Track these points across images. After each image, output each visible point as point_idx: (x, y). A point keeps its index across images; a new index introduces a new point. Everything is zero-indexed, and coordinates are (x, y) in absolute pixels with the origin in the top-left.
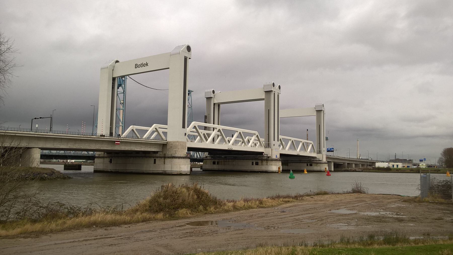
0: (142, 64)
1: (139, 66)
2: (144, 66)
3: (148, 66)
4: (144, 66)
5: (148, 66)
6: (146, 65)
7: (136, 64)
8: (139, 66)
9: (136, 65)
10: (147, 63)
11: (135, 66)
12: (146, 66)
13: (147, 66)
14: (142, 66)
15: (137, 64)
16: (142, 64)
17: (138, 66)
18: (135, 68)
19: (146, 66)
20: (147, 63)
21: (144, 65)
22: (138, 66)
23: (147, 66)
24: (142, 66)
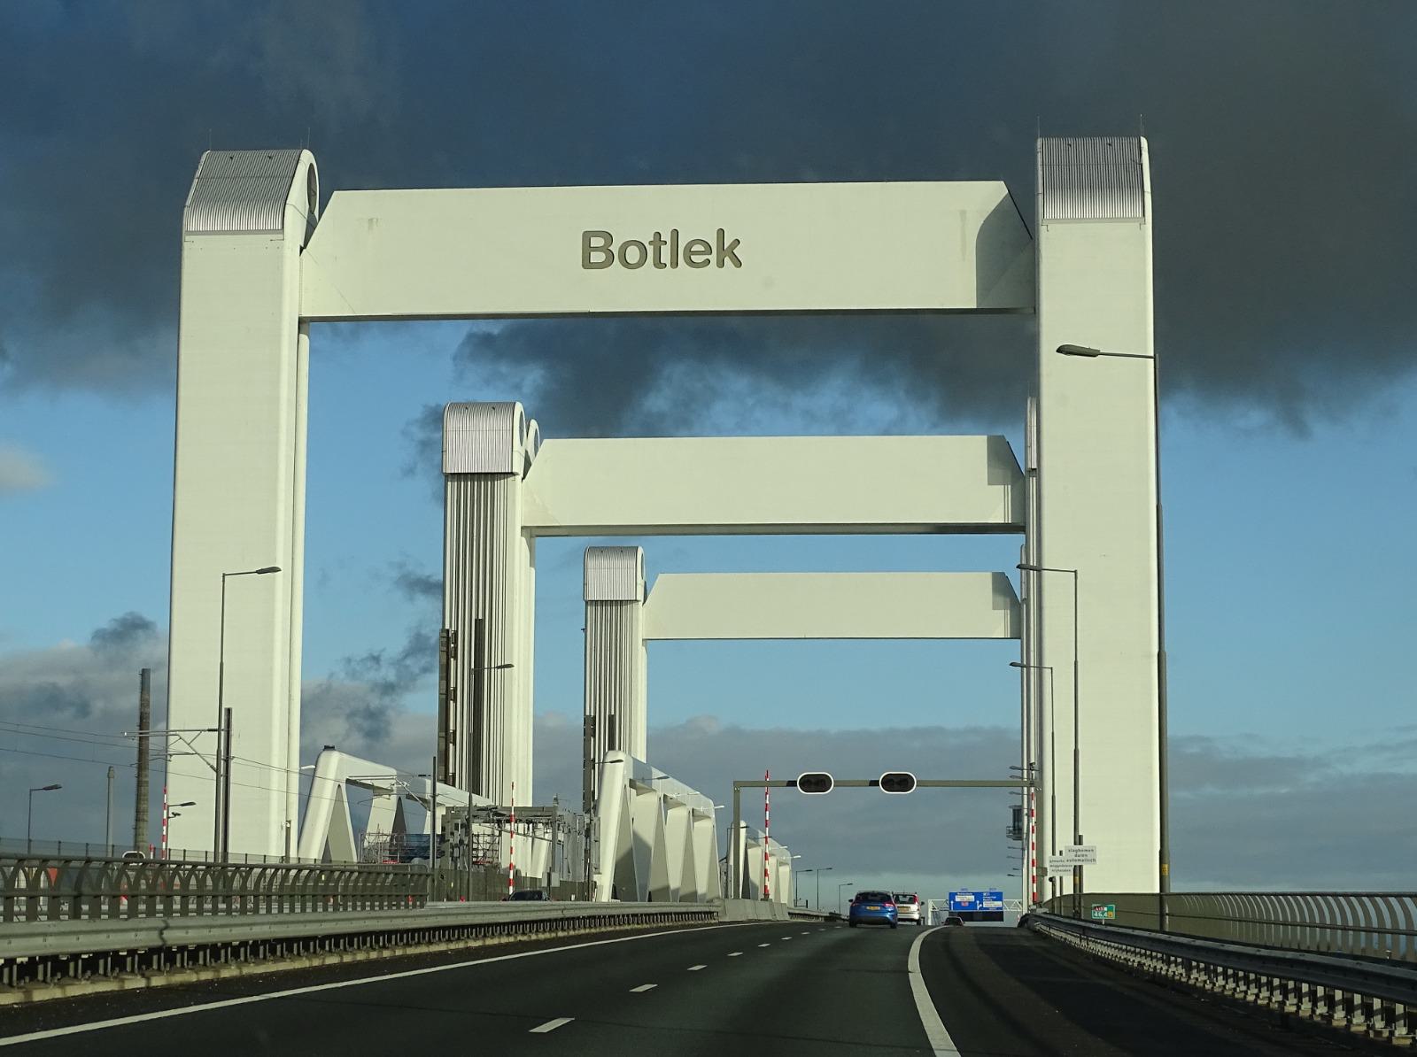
0: (666, 237)
1: (633, 255)
3: (738, 263)
5: (738, 263)
6: (713, 258)
7: (587, 236)
8: (633, 255)
9: (597, 242)
11: (587, 249)
12: (721, 264)
14: (666, 257)
15: (608, 237)
16: (666, 237)
17: (615, 248)
18: (587, 264)
19: (721, 264)
21: (689, 251)
22: (615, 248)
23: (727, 260)
24: (666, 257)
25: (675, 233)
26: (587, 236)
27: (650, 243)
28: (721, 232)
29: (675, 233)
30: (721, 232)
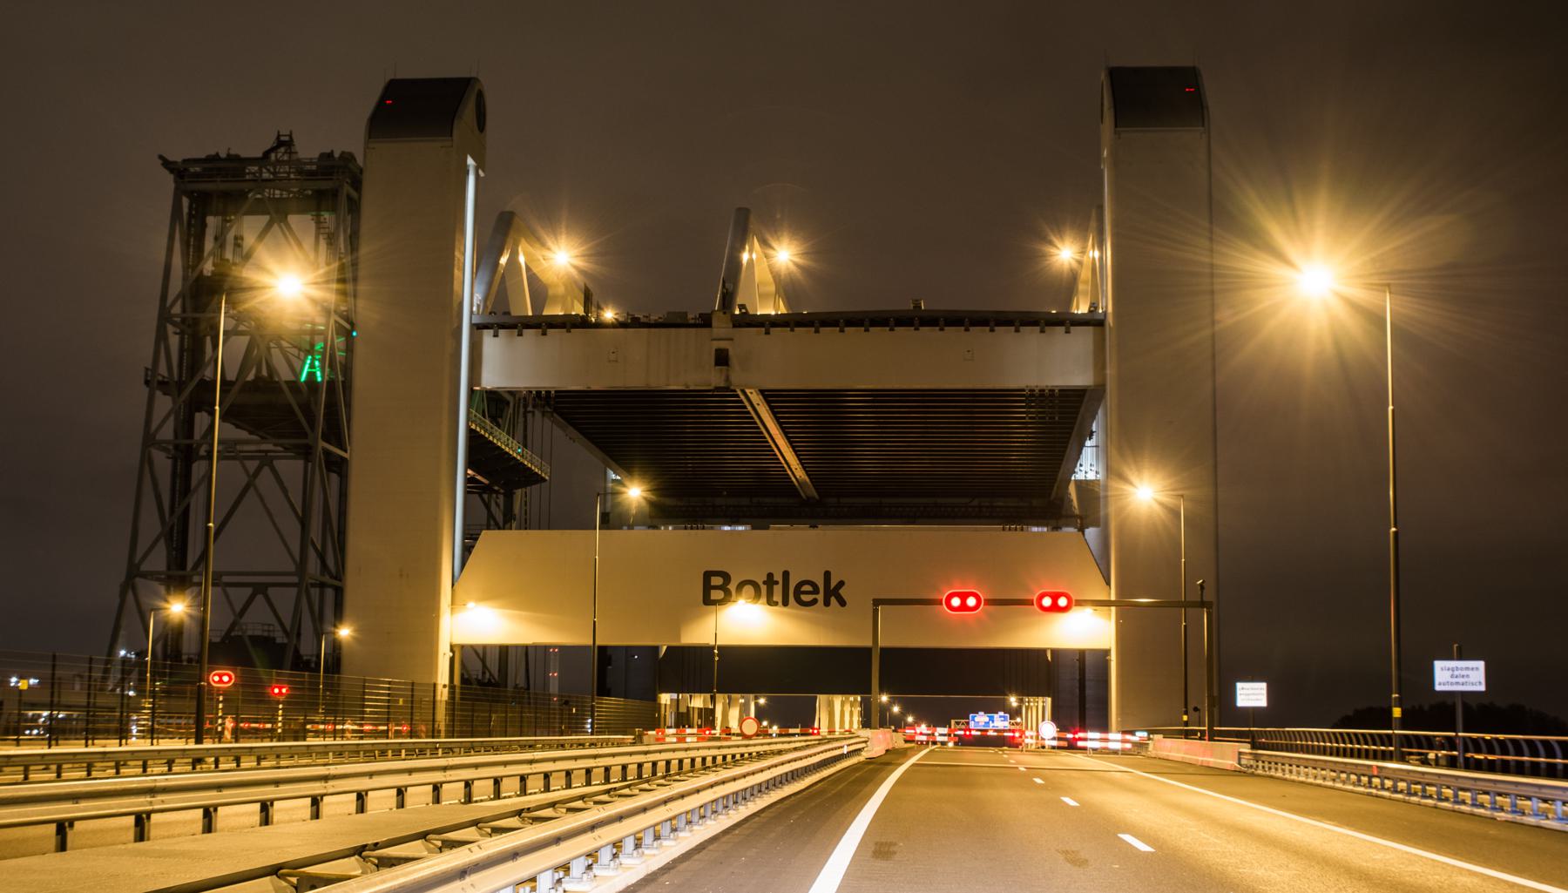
0: (778, 577)
2: (805, 598)
3: (842, 603)
4: (805, 598)
5: (842, 603)
6: (820, 597)
7: (708, 575)
10: (833, 584)
11: (707, 588)
12: (827, 603)
13: (833, 600)
14: (778, 590)
16: (778, 577)
19: (827, 603)
20: (833, 584)
21: (798, 592)
23: (833, 600)
25: (786, 575)
26: (708, 575)
27: (764, 583)
28: (827, 575)
29: (786, 575)
30: (827, 575)
